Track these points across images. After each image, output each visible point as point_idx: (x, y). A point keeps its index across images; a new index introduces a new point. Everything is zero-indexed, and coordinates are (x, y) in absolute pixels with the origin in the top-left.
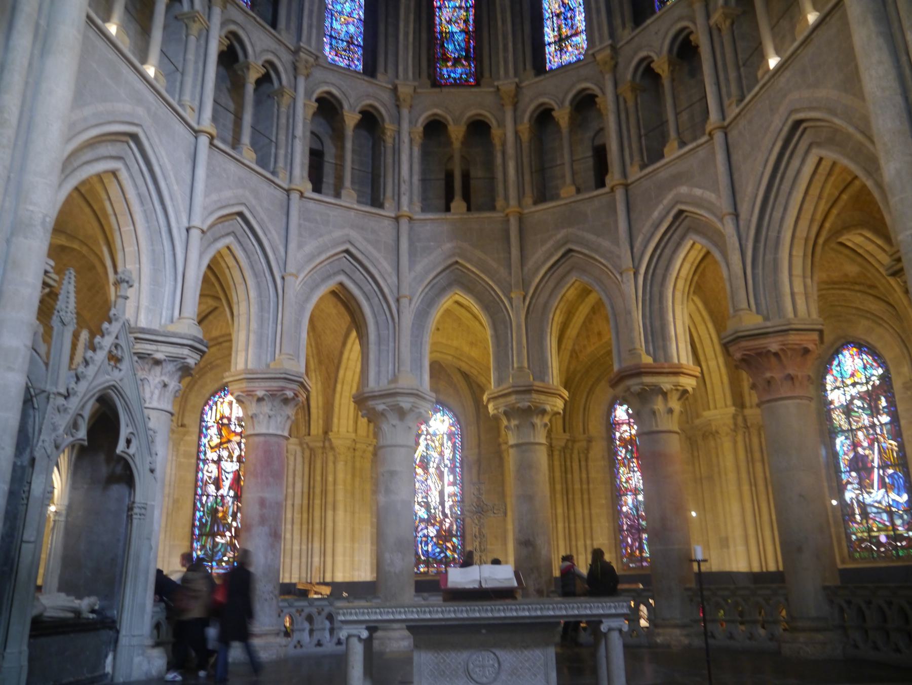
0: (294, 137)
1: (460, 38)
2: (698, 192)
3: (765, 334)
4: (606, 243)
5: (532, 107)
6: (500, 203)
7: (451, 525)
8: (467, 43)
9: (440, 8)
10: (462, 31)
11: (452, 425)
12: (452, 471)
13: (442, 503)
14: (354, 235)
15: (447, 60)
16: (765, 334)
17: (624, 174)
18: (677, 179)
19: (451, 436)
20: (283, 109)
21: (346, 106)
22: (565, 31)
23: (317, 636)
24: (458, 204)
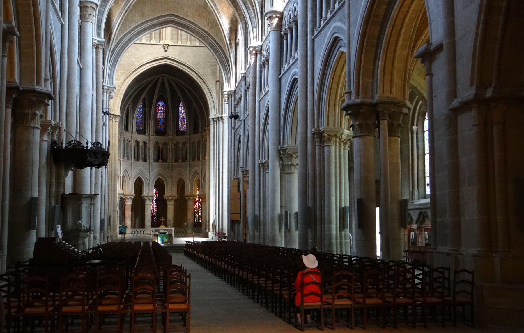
0: (132, 151)
1: (162, 120)
2: (198, 169)
3: (202, 195)
4: (185, 172)
5: (175, 142)
6: (168, 161)
7: (155, 214)
8: (163, 121)
9: (158, 112)
10: (162, 118)
11: (156, 191)
12: (156, 202)
13: (153, 209)
14: (142, 168)
15: (159, 125)
16: (202, 195)
17: (189, 162)
18: (196, 166)
19: (156, 194)
20: (130, 146)
21: (140, 142)
22: (183, 123)
23: (136, 234)
24: (160, 161)
